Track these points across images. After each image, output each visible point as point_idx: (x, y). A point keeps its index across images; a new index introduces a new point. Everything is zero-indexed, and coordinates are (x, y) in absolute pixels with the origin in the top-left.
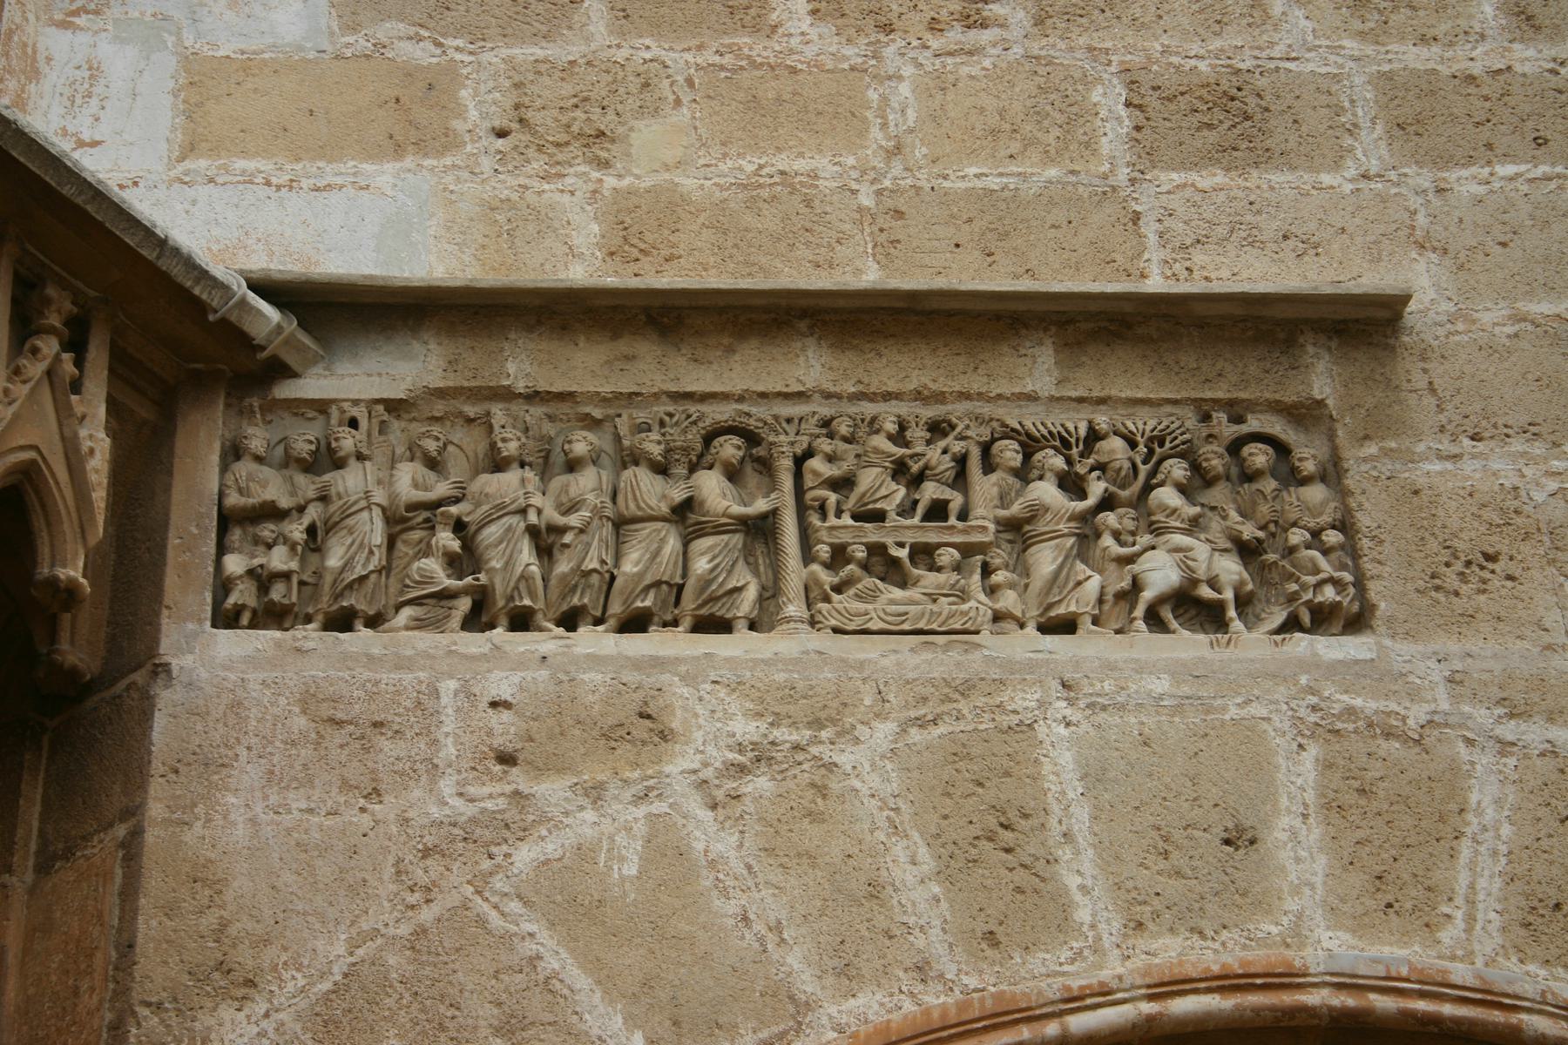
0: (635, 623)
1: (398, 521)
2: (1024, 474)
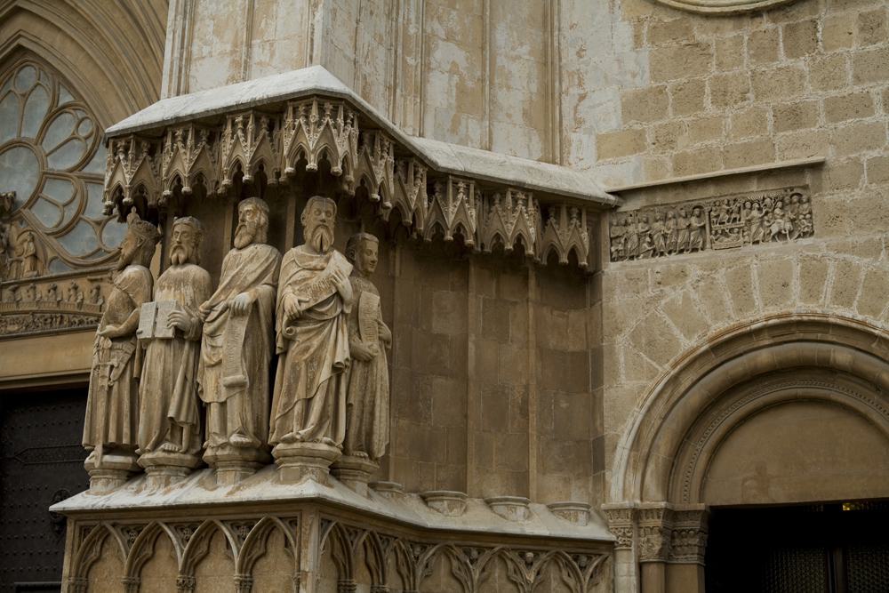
0: (681, 251)
1: (640, 236)
2: (751, 209)
